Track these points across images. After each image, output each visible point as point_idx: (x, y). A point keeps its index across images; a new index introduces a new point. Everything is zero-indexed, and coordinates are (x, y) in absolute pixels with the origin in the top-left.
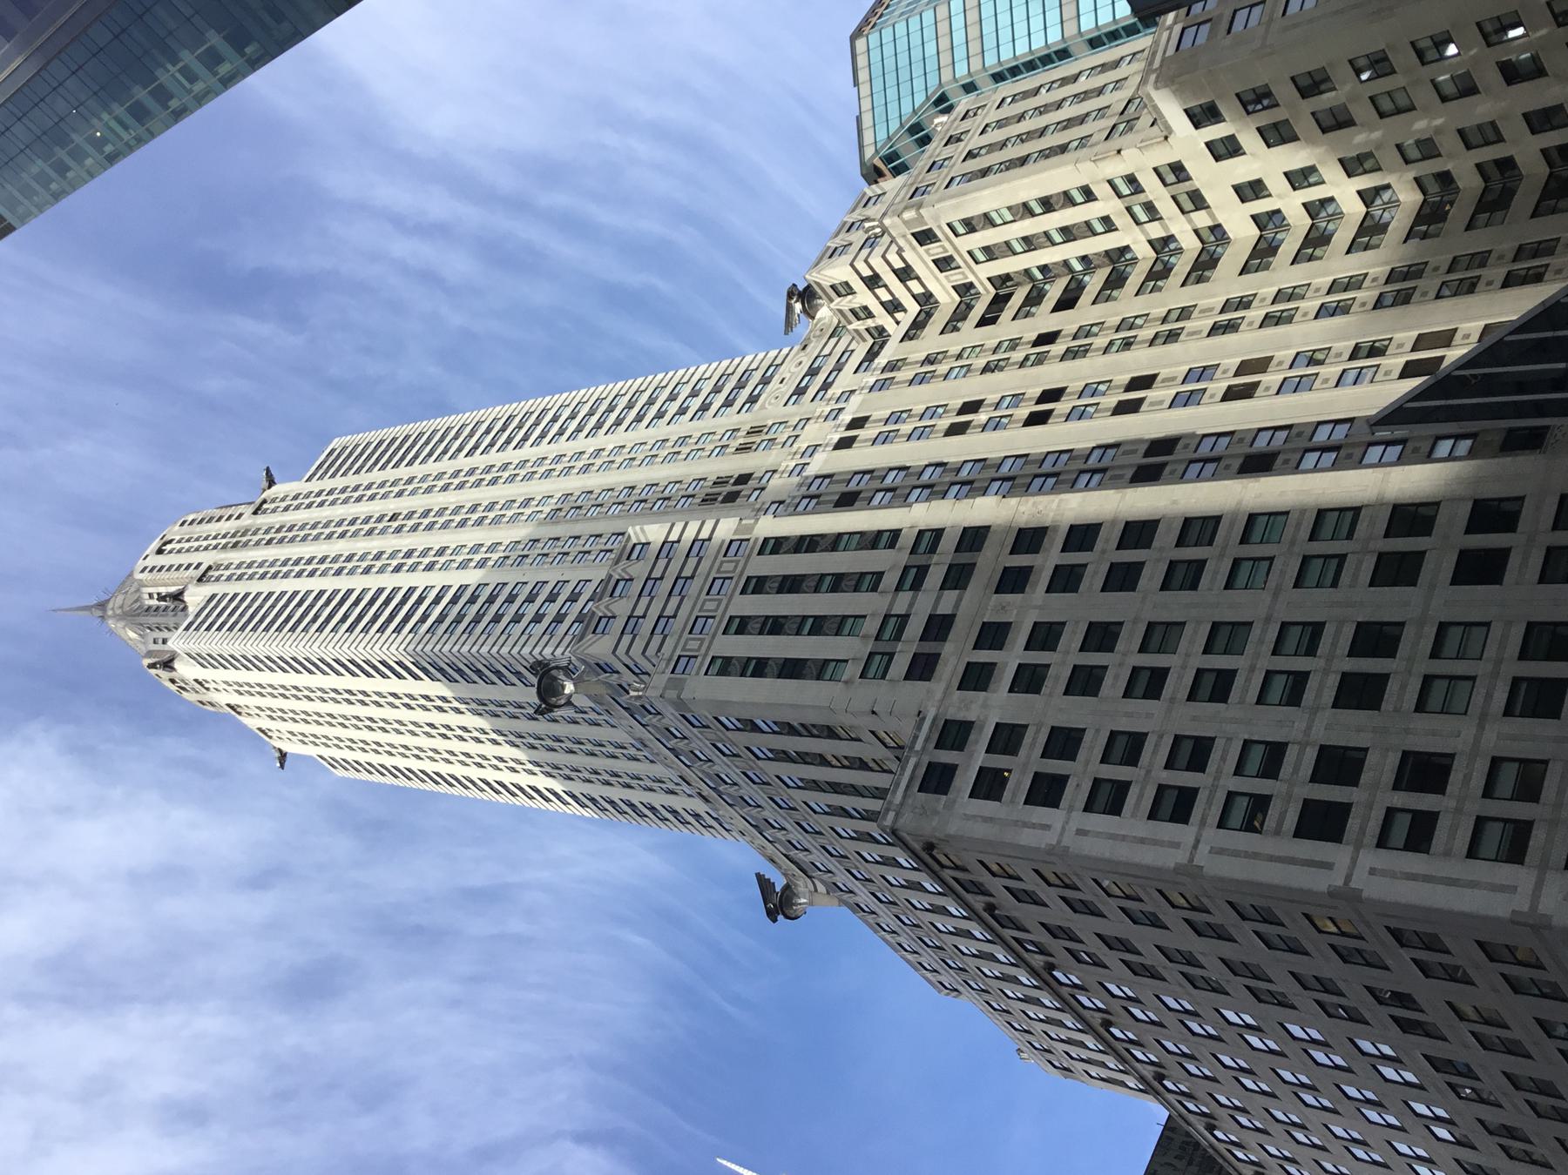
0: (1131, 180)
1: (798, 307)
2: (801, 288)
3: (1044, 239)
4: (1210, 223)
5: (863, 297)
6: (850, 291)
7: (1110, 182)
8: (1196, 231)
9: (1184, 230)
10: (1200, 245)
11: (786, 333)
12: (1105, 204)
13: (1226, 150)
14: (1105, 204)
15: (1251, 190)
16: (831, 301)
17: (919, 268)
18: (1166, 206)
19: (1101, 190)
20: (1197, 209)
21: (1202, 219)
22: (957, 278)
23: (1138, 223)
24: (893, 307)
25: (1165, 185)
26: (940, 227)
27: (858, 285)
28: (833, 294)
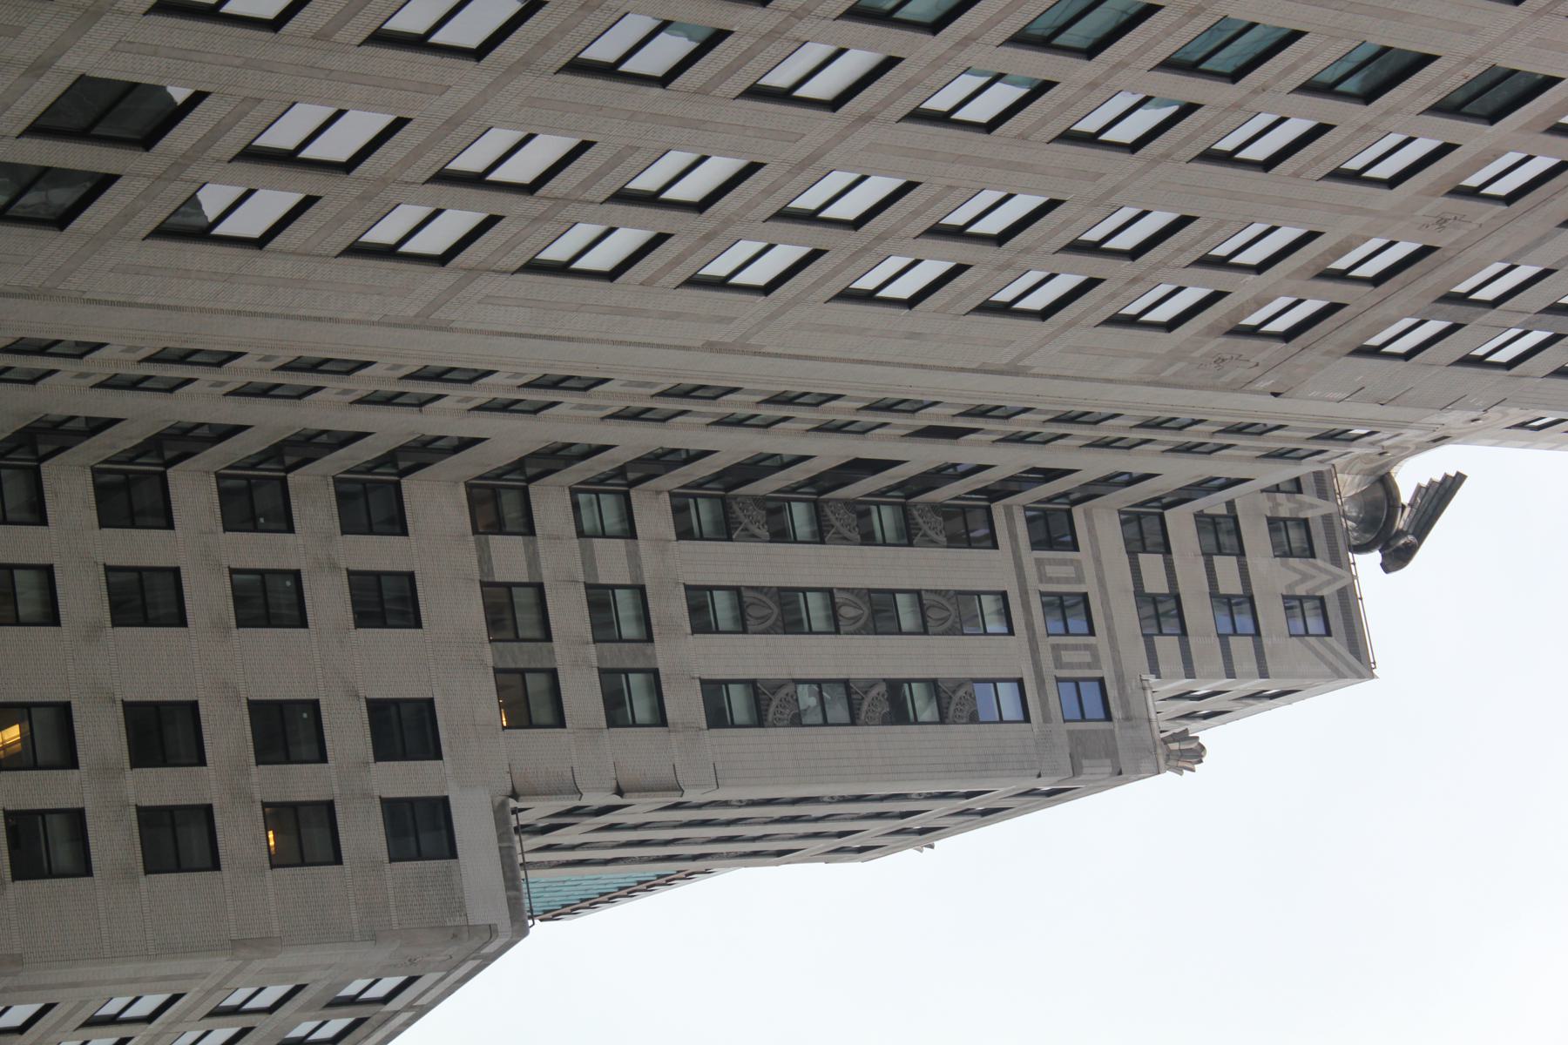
0: (616, 711)
1: (1401, 523)
2: (1375, 556)
3: (847, 612)
4: (496, 541)
5: (1272, 576)
6: (1293, 603)
7: (660, 719)
8: (529, 529)
9: (556, 555)
10: (533, 488)
11: (1459, 479)
12: (688, 658)
13: (405, 728)
14: (688, 658)
15: (386, 602)
16: (1327, 519)
17: (1124, 615)
18: (569, 614)
19: (685, 704)
20: (509, 586)
21: (509, 558)
22: (1059, 570)
23: (640, 591)
24: (1222, 534)
25: (553, 674)
26: (1047, 719)
27: (1271, 614)
28: (1317, 530)
